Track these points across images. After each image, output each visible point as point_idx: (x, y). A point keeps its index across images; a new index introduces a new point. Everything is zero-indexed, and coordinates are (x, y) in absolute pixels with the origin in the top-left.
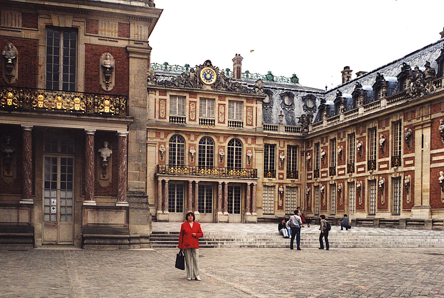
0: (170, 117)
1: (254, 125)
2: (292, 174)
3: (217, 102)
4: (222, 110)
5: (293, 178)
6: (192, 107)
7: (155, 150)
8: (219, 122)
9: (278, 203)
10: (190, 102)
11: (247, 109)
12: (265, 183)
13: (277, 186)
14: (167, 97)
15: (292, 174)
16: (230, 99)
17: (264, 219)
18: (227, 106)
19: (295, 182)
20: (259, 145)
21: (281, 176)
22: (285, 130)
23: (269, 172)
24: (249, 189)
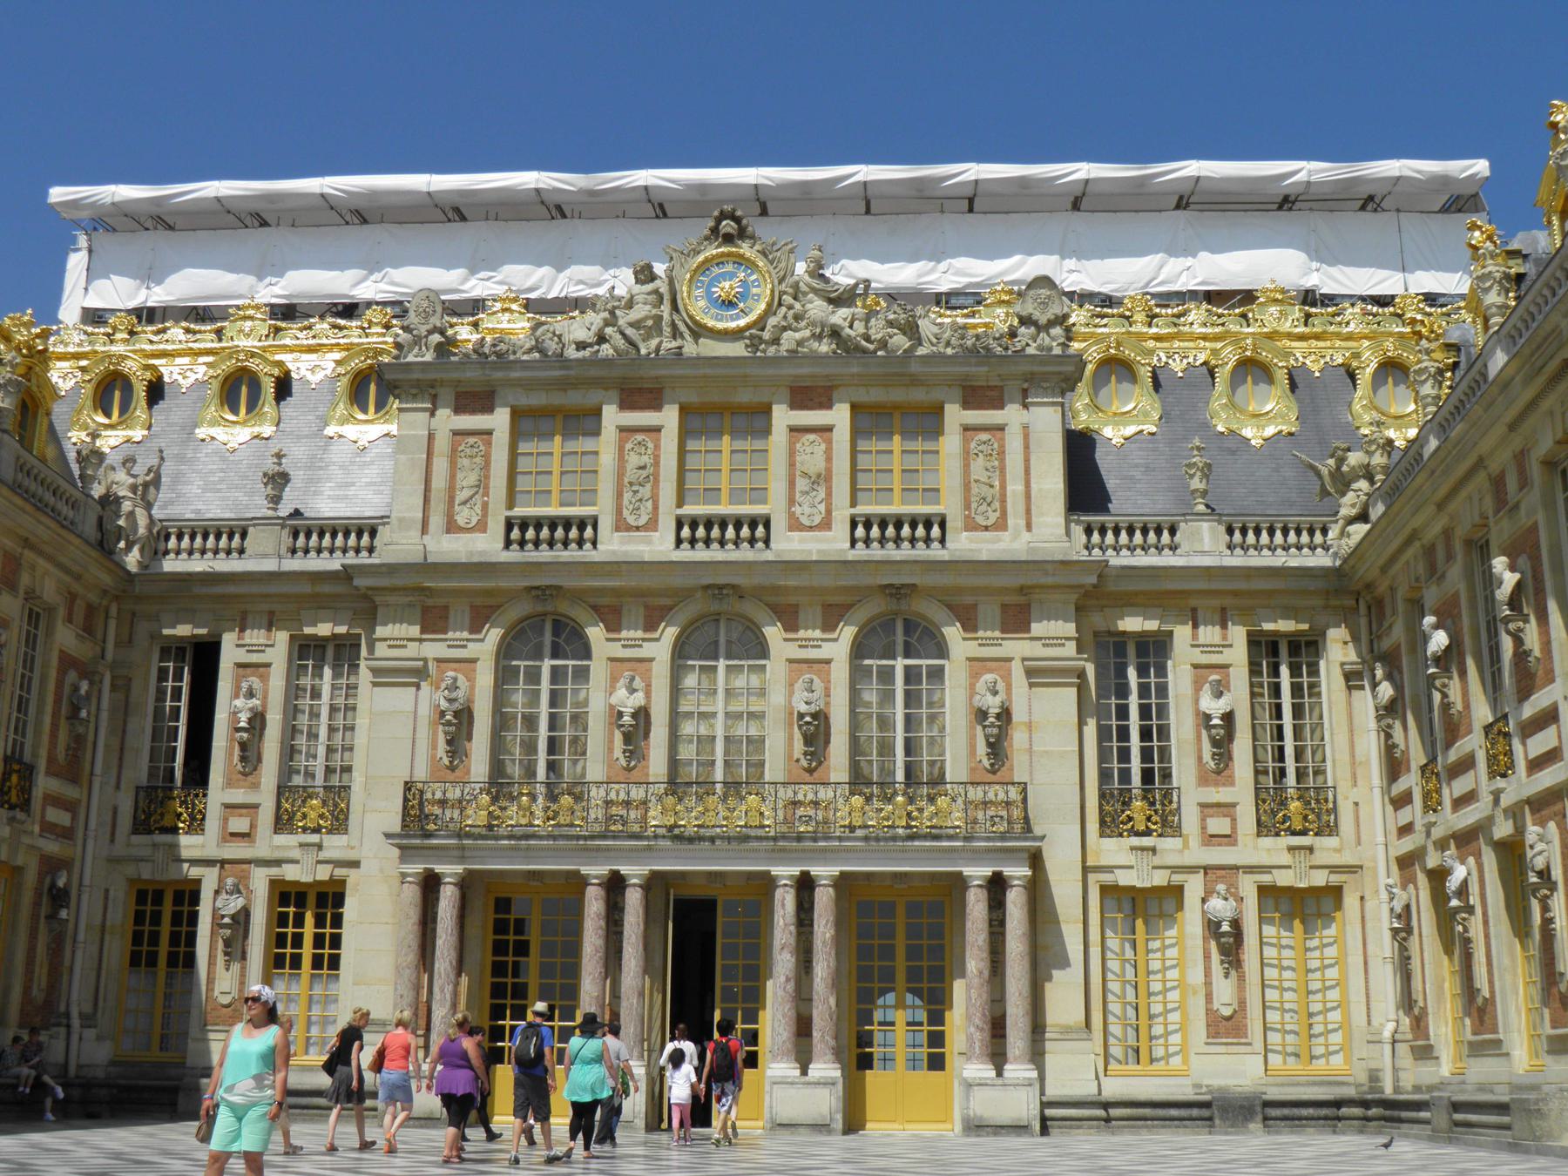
0: (509, 526)
1: (1015, 520)
2: (1295, 806)
3: (783, 417)
4: (811, 454)
5: (1304, 833)
6: (633, 460)
7: (410, 707)
8: (795, 525)
9: (1209, 997)
10: (626, 431)
11: (966, 442)
12: (1109, 869)
13: (1194, 887)
14: (499, 420)
15: (1295, 806)
16: (863, 396)
17: (1106, 1105)
18: (842, 434)
19: (1319, 858)
20: (1047, 641)
21: (1218, 825)
22: (1230, 547)
23: (1138, 804)
24: (976, 905)
